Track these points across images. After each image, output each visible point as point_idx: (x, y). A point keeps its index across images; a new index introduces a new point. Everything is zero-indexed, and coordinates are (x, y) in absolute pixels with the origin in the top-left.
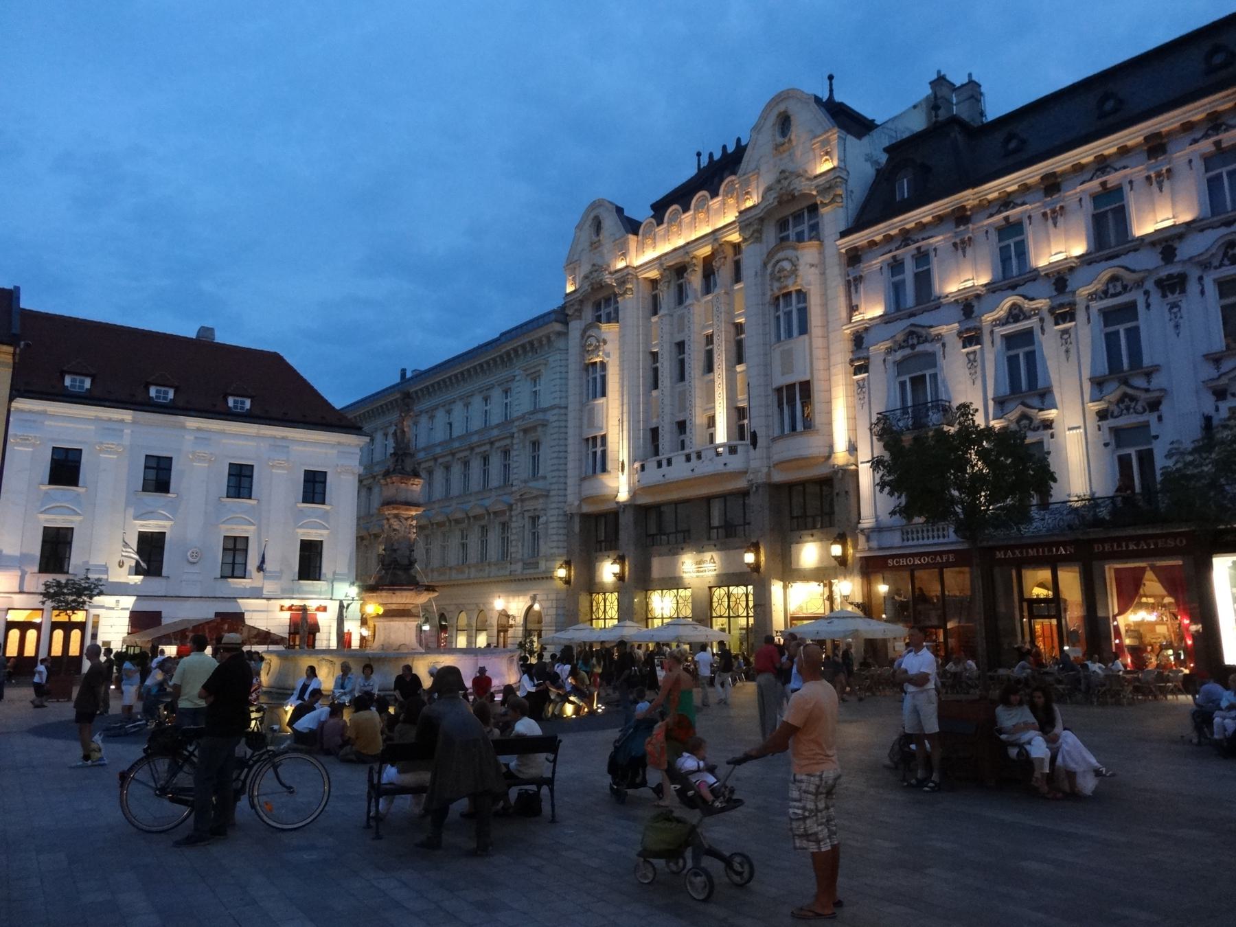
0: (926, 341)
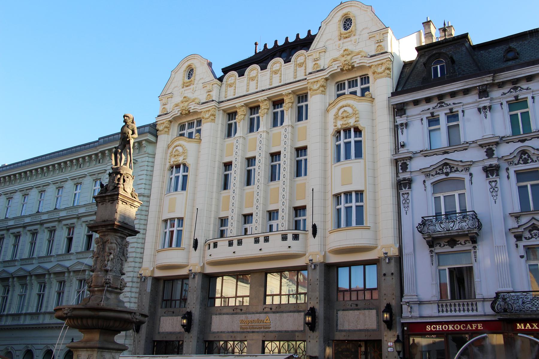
0: (457, 170)
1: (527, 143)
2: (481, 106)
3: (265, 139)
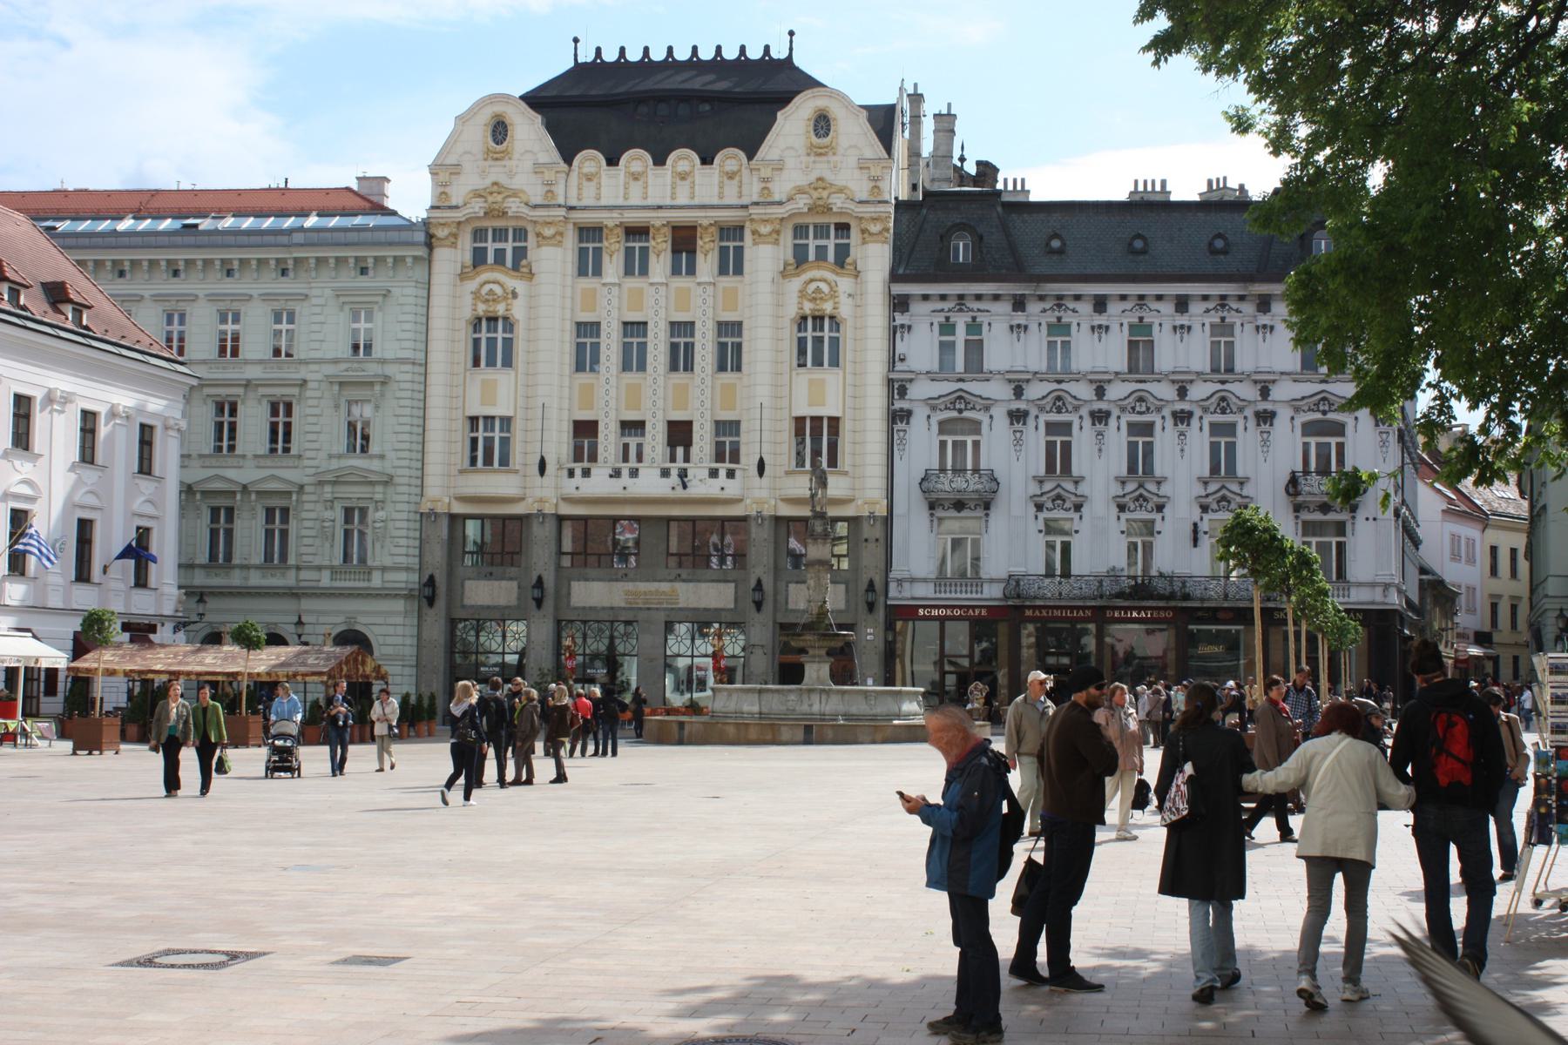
0: (973, 408)
1: (1063, 386)
2: (1015, 322)
3: (660, 296)
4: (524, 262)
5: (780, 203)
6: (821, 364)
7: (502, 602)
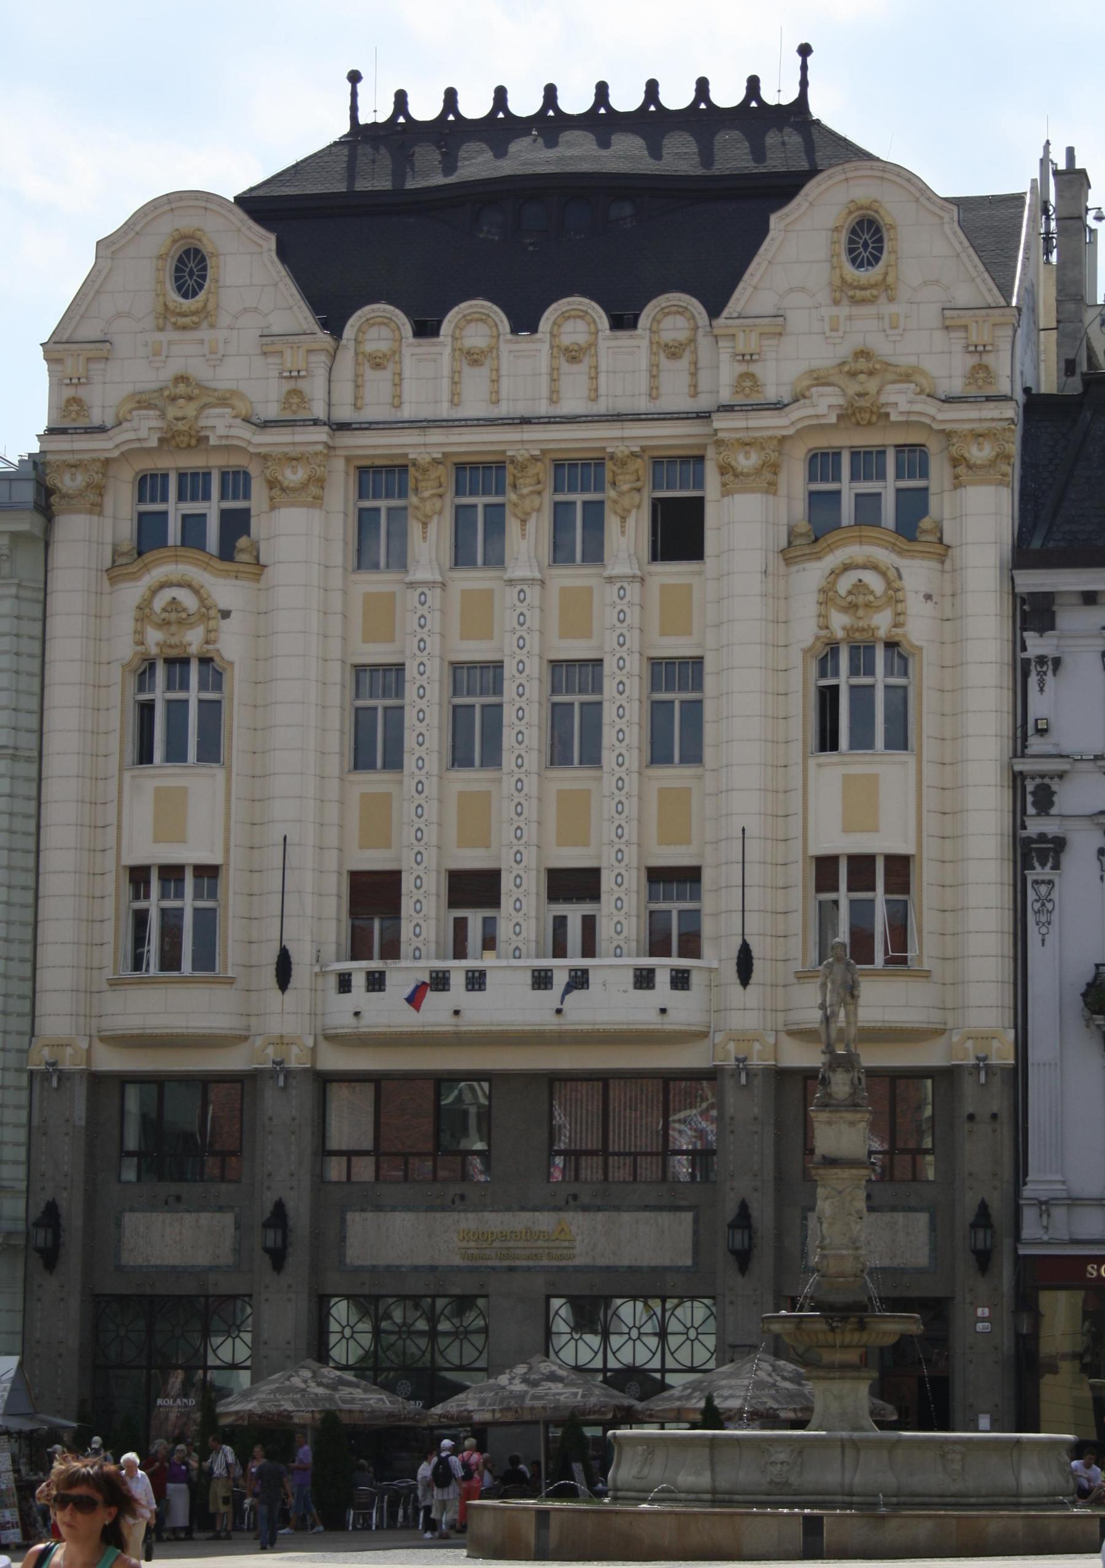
3: (529, 607)
4: (243, 542)
5: (778, 406)
6: (869, 744)
7: (202, 1259)
